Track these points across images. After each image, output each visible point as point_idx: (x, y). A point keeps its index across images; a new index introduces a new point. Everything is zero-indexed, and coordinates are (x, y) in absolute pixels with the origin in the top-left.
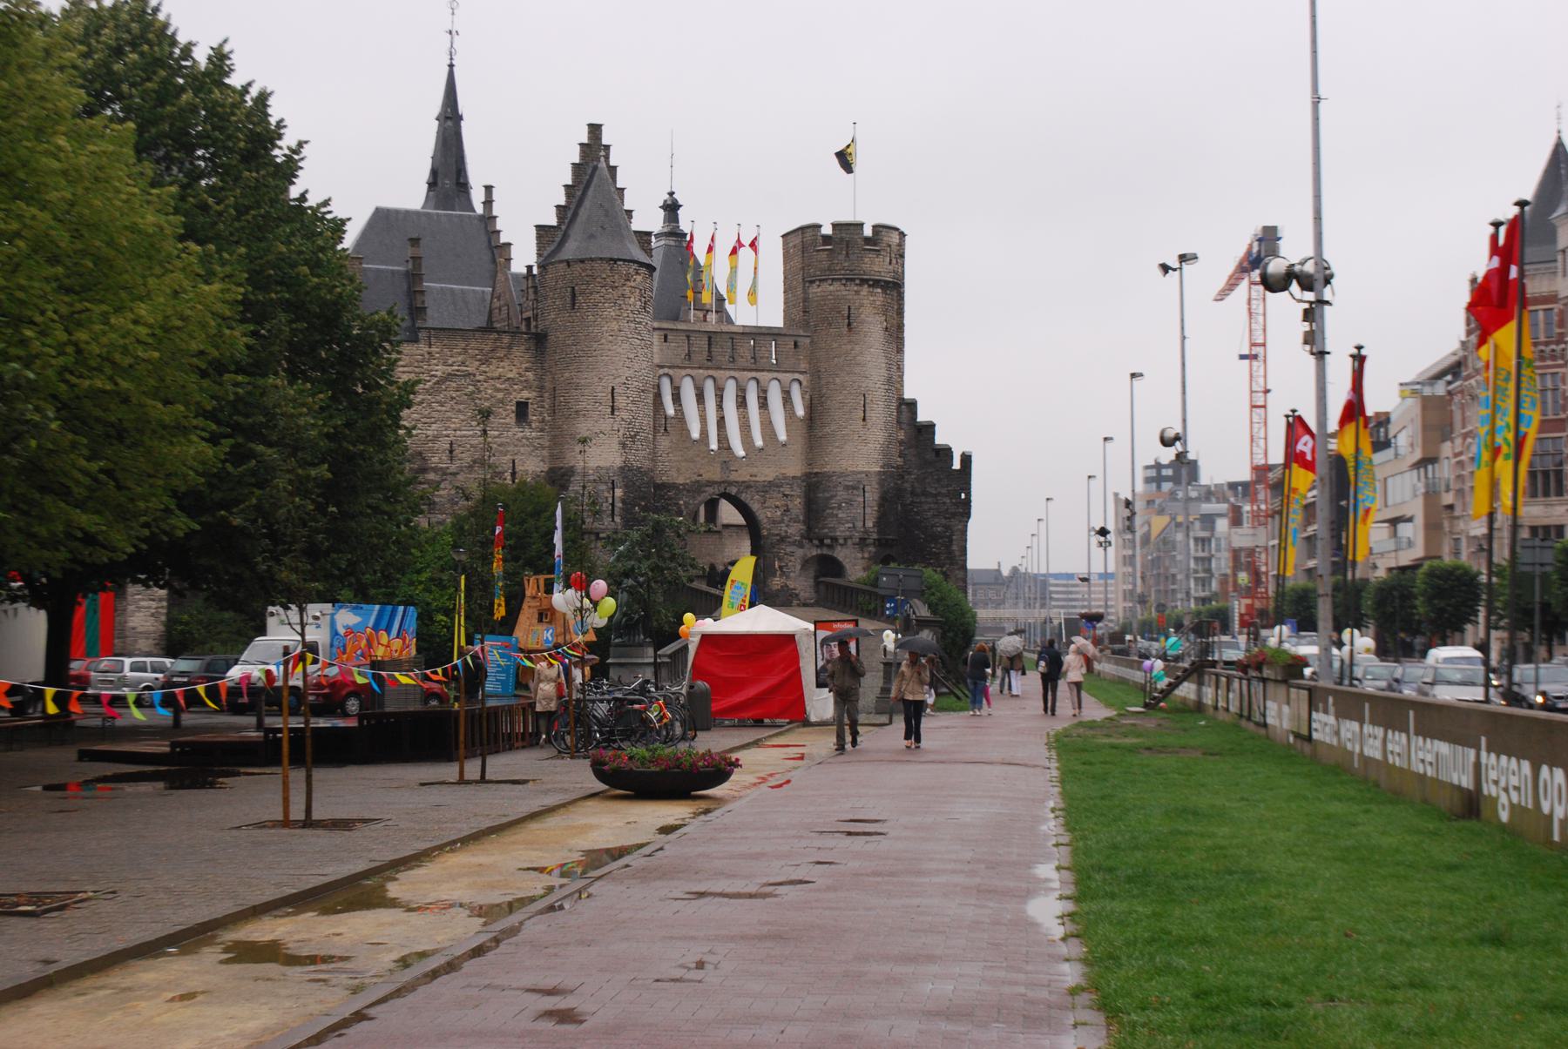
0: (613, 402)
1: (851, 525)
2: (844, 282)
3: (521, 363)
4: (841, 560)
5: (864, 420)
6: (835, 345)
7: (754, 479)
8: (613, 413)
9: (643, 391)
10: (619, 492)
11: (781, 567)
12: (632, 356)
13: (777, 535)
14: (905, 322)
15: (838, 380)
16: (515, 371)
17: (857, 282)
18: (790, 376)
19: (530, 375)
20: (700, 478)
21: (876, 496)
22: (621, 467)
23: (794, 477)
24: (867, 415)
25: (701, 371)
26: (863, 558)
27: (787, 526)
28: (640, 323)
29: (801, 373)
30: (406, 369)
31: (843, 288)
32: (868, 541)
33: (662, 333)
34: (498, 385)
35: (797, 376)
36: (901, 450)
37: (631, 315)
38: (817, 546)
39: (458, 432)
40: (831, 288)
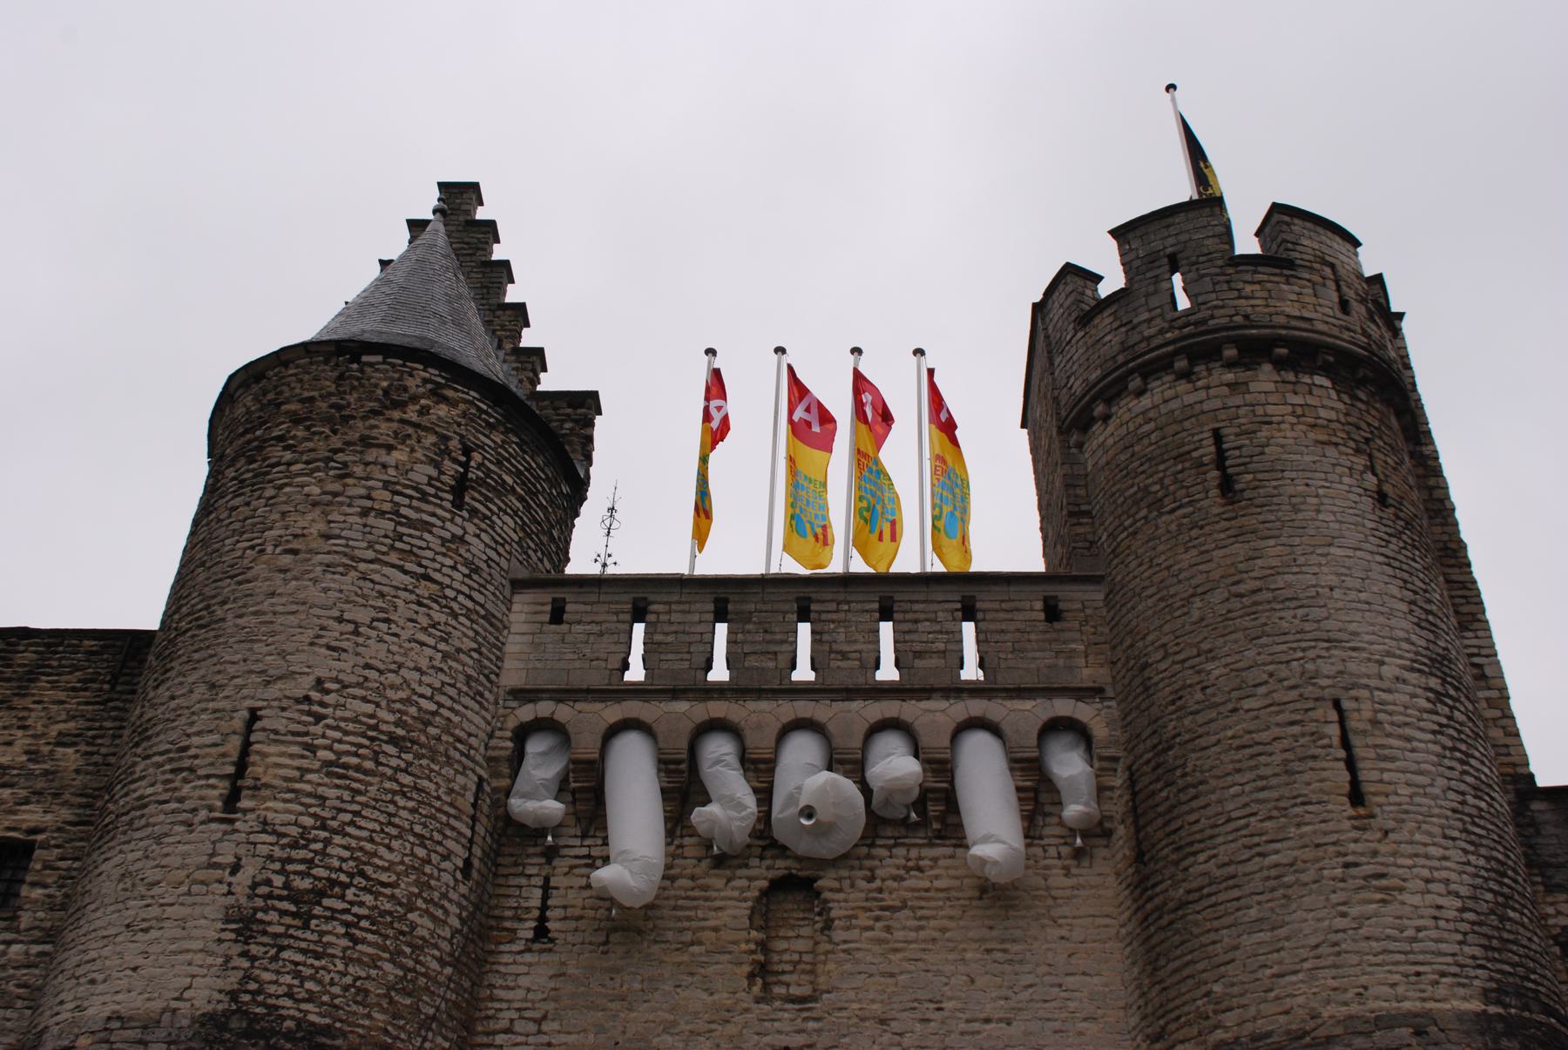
2: (1181, 364)
3: (52, 720)
5: (1356, 796)
6: (1187, 558)
9: (393, 740)
12: (363, 616)
14: (1466, 534)
15: (1215, 669)
16: (22, 741)
17: (1230, 352)
18: (1035, 711)
19: (69, 757)
24: (1367, 774)
25: (682, 706)
28: (427, 527)
29: (1081, 693)
31: (1183, 386)
33: (546, 596)
35: (1063, 707)
37: (387, 495)
40: (1146, 401)
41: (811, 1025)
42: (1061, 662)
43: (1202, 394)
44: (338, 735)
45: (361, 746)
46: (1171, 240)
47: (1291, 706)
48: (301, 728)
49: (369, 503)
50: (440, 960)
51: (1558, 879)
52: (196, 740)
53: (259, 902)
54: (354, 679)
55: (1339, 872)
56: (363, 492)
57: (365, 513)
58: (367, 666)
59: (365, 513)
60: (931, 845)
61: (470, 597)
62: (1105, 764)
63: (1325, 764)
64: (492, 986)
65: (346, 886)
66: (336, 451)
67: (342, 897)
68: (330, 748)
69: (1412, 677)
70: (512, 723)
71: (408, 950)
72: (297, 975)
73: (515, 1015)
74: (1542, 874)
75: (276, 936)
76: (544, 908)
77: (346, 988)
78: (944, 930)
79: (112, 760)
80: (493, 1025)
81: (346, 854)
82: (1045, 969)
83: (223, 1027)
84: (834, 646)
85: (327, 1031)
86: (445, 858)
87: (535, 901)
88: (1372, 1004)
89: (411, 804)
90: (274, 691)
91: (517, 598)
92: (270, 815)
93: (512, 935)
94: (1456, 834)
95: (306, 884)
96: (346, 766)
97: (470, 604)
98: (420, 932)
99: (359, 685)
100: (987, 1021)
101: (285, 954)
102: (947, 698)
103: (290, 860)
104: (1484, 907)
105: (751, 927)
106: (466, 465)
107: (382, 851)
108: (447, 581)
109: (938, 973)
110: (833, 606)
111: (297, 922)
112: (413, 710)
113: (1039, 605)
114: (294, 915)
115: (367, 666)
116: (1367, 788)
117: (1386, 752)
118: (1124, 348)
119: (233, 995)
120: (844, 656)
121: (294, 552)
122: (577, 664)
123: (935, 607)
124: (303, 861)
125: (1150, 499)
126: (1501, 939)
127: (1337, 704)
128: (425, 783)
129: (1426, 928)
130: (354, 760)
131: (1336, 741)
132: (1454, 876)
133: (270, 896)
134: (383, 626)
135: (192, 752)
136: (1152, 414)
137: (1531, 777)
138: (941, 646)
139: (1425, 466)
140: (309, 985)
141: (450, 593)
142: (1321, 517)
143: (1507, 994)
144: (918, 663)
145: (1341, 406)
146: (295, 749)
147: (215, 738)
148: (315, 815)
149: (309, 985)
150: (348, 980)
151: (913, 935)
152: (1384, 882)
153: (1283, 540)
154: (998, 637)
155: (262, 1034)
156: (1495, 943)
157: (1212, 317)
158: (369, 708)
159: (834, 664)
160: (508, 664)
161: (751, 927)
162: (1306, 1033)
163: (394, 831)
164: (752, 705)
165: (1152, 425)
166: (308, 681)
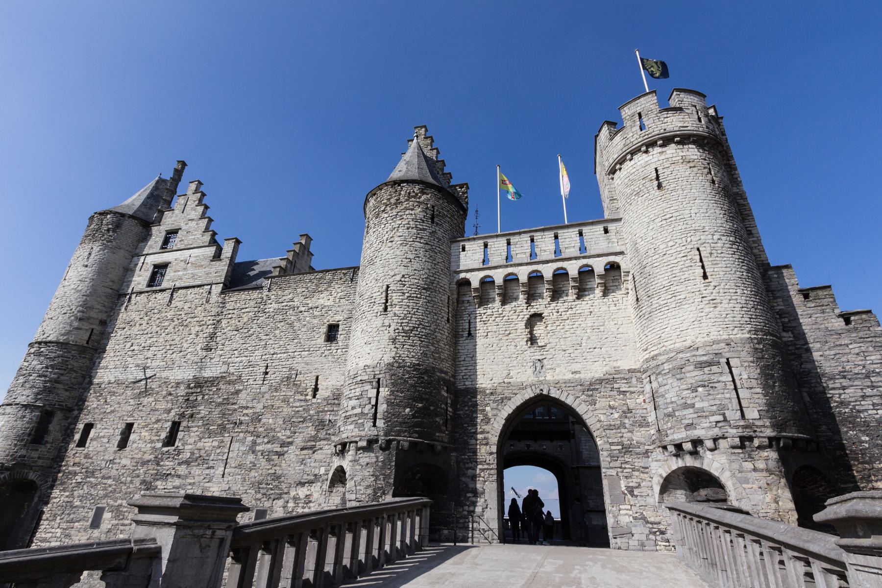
0: (387, 301)
1: (721, 418)
4: (716, 473)
5: (705, 277)
7: (577, 376)
8: (386, 309)
10: (384, 392)
11: (631, 490)
12: (412, 257)
13: (618, 444)
16: (332, 299)
20: (506, 380)
21: (755, 372)
22: (389, 364)
23: (629, 371)
26: (755, 470)
27: (631, 432)
28: (424, 230)
29: (616, 254)
30: (247, 310)
31: (645, 155)
32: (756, 442)
34: (315, 313)
36: (783, 323)
38: (677, 456)
39: (275, 356)
40: (633, 162)
41: (545, 353)
42: (610, 245)
43: (651, 157)
44: (410, 289)
45: (416, 291)
46: (639, 108)
47: (683, 252)
48: (401, 288)
49: (409, 226)
50: (444, 344)
51: (778, 295)
52: (374, 295)
53: (397, 334)
54: (411, 274)
55: (700, 300)
56: (407, 222)
57: (408, 228)
58: (415, 270)
59: (408, 228)
60: (574, 301)
61: (439, 247)
62: (625, 274)
63: (695, 268)
64: (459, 350)
65: (417, 328)
66: (398, 212)
67: (417, 331)
68: (408, 293)
69: (724, 238)
70: (455, 280)
71: (436, 342)
72: (409, 351)
73: (465, 356)
74: (772, 294)
75: (402, 342)
76: (470, 328)
77: (421, 354)
78: (580, 325)
79: (354, 301)
80: (460, 359)
81: (416, 320)
82: (611, 333)
83: (393, 366)
84: (542, 249)
85: (418, 365)
86: (442, 318)
87: (467, 327)
88: (712, 337)
89: (431, 305)
90: (391, 280)
91: (452, 246)
92: (396, 312)
93: (462, 336)
94: (740, 285)
95: (407, 328)
96: (413, 297)
97: (439, 249)
98: (438, 338)
99: (413, 275)
100: (595, 348)
101: (405, 347)
102: (576, 260)
103: (402, 323)
104: (750, 306)
105: (526, 328)
106: (433, 211)
107: (426, 318)
108: (433, 244)
109: (579, 336)
110: (541, 237)
111: (407, 338)
112: (429, 280)
113: (602, 229)
114: (406, 336)
115: (415, 270)
116: (708, 274)
117: (713, 262)
118: (625, 145)
119: (394, 358)
120: (545, 251)
121: (392, 242)
122: (471, 262)
123: (570, 234)
124: (406, 323)
125: (635, 193)
126: (756, 315)
127: (698, 249)
128: (434, 299)
129: (729, 314)
130: (415, 295)
131: (698, 260)
132: (739, 297)
133: (399, 333)
134: (417, 258)
135: (374, 298)
136: (634, 166)
137: (769, 264)
138: (573, 245)
139: (731, 168)
140: (412, 354)
141: (434, 247)
142: (692, 191)
143: (758, 331)
144: (567, 251)
145: (699, 154)
146: (401, 294)
147: (379, 293)
148: (407, 311)
149: (412, 354)
150: (421, 351)
151: (571, 327)
152: (715, 301)
153: (680, 200)
154: (590, 240)
155: (404, 367)
156: (753, 317)
157: (654, 131)
158: (416, 281)
159: (542, 254)
160: (452, 264)
161: (526, 328)
162: (691, 346)
163: (428, 313)
164: (520, 268)
165: (635, 169)
166: (401, 276)
